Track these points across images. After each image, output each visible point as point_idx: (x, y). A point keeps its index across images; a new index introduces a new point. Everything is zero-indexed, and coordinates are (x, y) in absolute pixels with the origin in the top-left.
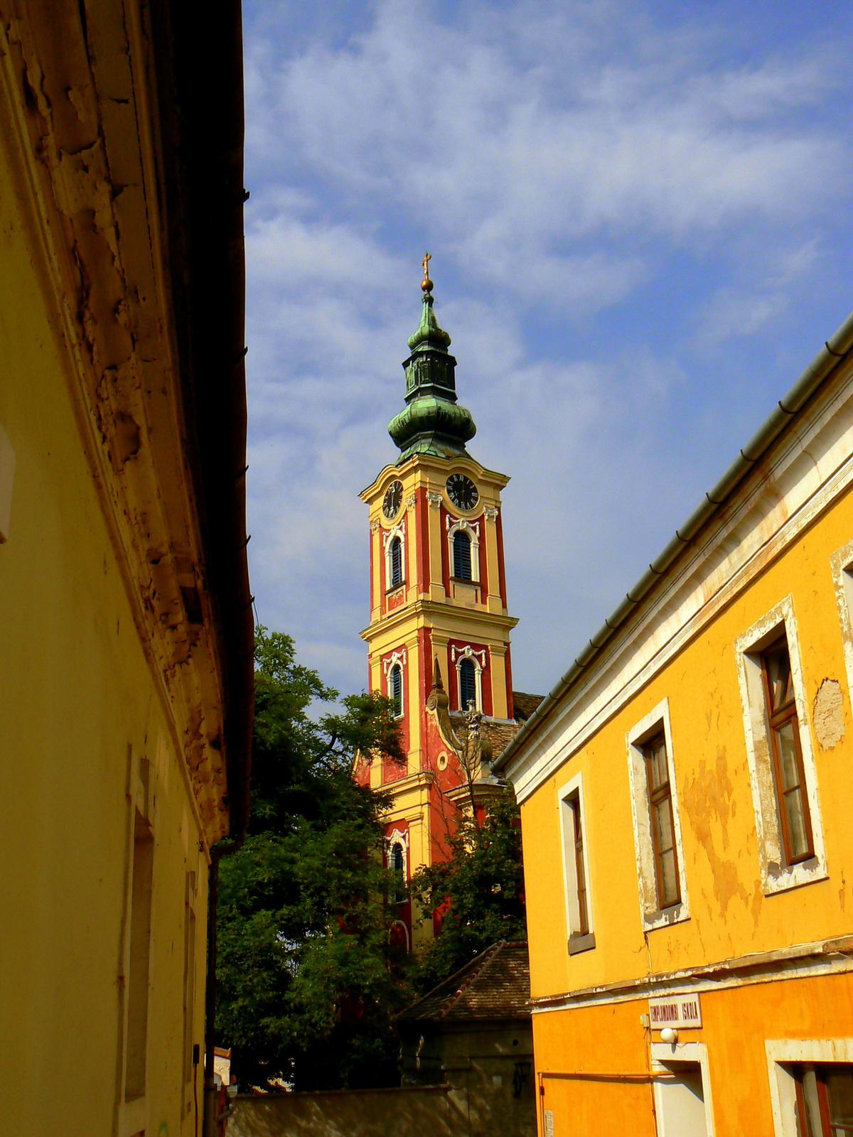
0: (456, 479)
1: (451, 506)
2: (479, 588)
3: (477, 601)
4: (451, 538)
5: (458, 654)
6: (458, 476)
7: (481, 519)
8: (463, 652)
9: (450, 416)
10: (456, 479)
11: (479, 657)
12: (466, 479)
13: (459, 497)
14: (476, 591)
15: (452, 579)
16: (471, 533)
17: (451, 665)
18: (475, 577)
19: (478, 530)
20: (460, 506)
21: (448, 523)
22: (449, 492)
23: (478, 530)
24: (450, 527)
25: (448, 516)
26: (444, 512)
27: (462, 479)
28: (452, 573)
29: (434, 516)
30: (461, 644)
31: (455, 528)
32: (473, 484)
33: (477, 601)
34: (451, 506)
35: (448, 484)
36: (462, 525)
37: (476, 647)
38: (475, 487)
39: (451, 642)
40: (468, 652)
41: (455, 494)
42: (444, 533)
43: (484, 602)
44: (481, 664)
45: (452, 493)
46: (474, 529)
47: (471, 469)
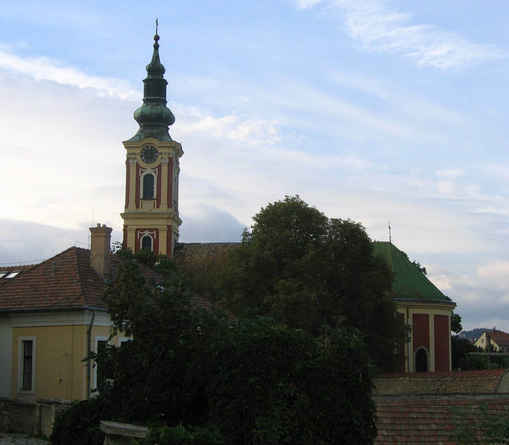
0: (146, 149)
1: (142, 164)
2: (156, 201)
3: (154, 208)
4: (142, 179)
5: (141, 235)
6: (147, 147)
7: (160, 167)
8: (144, 234)
9: (149, 115)
10: (146, 149)
11: (153, 235)
12: (152, 147)
13: (147, 158)
14: (154, 203)
15: (141, 199)
16: (154, 174)
17: (137, 241)
18: (155, 196)
19: (157, 172)
20: (147, 162)
21: (140, 172)
22: (141, 156)
23: (157, 172)
24: (141, 174)
25: (140, 169)
26: (138, 166)
27: (150, 148)
28: (141, 196)
29: (133, 170)
30: (143, 230)
31: (144, 174)
32: (156, 149)
33: (154, 208)
34: (142, 164)
35: (141, 152)
36: (149, 171)
37: (151, 230)
38: (157, 150)
39: (137, 230)
40: (147, 233)
41: (145, 157)
42: (138, 178)
43: (158, 207)
44: (153, 237)
45: (144, 157)
46: (155, 172)
47: (152, 142)
